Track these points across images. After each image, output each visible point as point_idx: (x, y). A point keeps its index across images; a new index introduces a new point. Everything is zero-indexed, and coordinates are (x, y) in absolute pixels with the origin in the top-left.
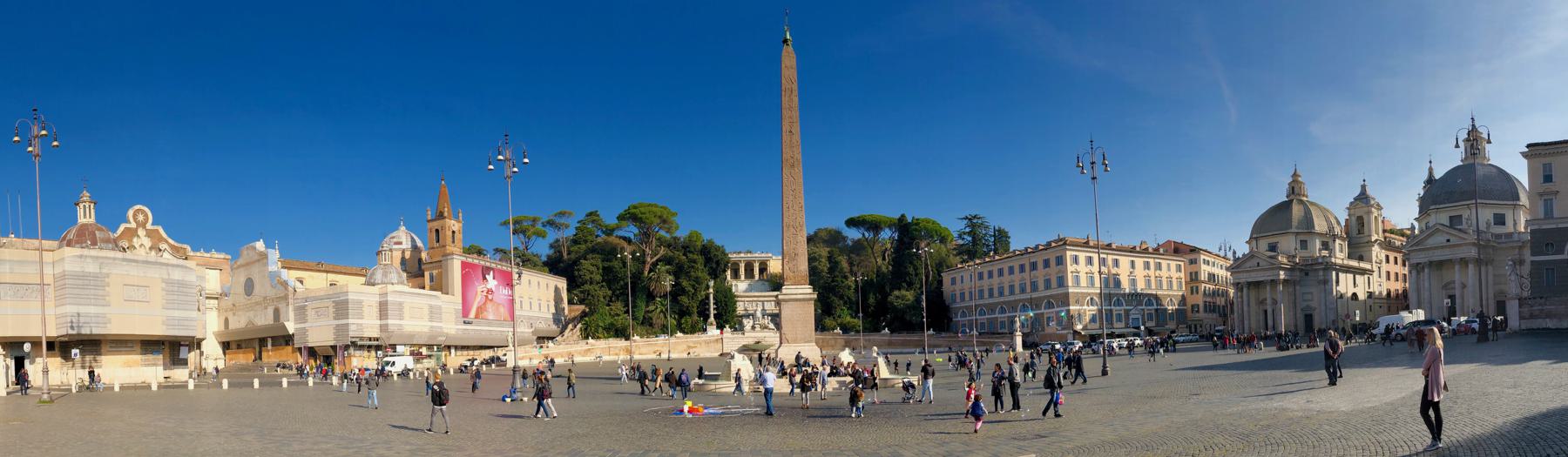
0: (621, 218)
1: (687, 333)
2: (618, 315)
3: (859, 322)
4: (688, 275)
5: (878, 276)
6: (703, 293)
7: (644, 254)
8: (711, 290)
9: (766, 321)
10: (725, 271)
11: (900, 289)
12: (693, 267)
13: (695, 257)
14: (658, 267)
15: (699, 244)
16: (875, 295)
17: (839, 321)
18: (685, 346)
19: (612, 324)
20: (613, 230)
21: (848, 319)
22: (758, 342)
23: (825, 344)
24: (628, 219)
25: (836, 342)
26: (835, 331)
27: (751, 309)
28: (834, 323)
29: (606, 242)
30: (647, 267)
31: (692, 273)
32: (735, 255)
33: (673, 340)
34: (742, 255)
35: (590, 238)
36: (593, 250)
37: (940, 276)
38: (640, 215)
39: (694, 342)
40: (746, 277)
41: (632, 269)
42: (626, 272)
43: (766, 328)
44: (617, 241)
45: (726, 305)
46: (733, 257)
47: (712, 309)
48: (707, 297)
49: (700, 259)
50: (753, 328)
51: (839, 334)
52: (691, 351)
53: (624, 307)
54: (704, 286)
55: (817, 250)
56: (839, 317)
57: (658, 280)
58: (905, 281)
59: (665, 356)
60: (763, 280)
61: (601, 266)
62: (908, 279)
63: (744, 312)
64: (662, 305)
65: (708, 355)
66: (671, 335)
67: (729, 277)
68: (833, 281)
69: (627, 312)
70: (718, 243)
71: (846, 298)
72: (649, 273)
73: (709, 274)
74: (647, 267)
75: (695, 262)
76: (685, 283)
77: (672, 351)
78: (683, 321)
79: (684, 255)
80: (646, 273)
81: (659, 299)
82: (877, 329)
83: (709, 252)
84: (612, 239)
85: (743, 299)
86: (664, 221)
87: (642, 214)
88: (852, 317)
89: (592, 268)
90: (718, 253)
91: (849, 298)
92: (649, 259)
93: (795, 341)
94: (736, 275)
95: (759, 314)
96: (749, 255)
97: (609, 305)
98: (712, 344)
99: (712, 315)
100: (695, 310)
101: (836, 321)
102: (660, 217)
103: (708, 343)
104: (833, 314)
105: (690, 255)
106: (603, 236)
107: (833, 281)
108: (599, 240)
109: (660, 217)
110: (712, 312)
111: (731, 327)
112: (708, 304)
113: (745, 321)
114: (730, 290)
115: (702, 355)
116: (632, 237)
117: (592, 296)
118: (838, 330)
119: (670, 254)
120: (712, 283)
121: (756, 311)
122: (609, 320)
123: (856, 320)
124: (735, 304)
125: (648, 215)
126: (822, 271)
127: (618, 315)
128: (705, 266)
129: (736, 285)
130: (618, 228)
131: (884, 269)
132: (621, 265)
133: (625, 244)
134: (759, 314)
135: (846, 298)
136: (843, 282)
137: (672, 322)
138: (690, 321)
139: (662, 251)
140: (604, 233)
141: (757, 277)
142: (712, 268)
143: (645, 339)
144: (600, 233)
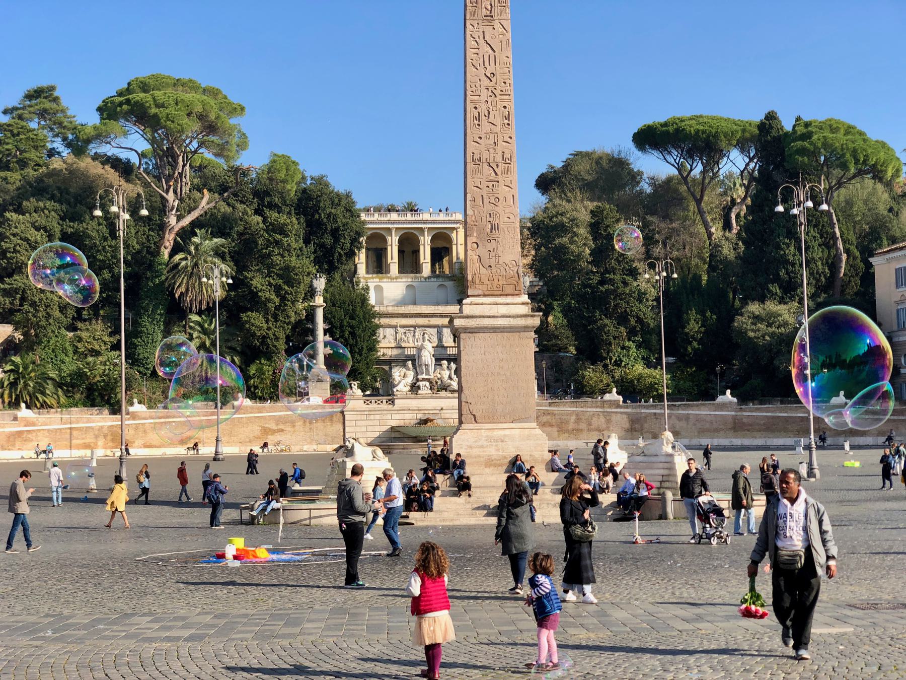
0: (108, 111)
1: (262, 399)
2: (97, 353)
3: (662, 377)
4: (264, 259)
5: (712, 268)
6: (300, 306)
7: (161, 208)
8: (319, 300)
9: (446, 374)
10: (351, 254)
11: (762, 300)
12: (278, 243)
13: (283, 219)
14: (196, 240)
15: (292, 188)
16: (703, 313)
17: (617, 374)
18: (256, 429)
19: (79, 375)
20: (88, 141)
21: (640, 368)
22: (425, 422)
23: (583, 426)
24: (126, 116)
25: (609, 421)
26: (607, 397)
27: (410, 343)
28: (606, 379)
29: (73, 173)
30: (169, 239)
31: (277, 259)
32: (376, 216)
33: (226, 413)
34: (394, 216)
35: (32, 155)
36: (39, 189)
37: (869, 266)
38: (153, 110)
39: (278, 420)
40: (402, 270)
41: (133, 242)
42: (116, 249)
43: (445, 388)
44: (95, 169)
45: (353, 334)
46: (372, 221)
48: (311, 316)
49: (295, 224)
50: (414, 388)
51: (615, 404)
52: (271, 440)
53: (111, 335)
54: (302, 288)
55: (568, 207)
56: (618, 364)
57: (194, 273)
58: (777, 279)
59: (207, 450)
60: (442, 276)
61: (57, 230)
62: (782, 273)
63: (396, 352)
64: (204, 331)
65: (309, 448)
66: (224, 403)
67: (362, 269)
68: (602, 282)
69: (116, 347)
70: (338, 185)
71: (633, 322)
72: (172, 255)
73: (317, 261)
74: (169, 239)
75: (282, 230)
76: (258, 282)
77: (224, 439)
78: (252, 370)
79: (258, 212)
80: (166, 253)
81: (195, 318)
82: (708, 395)
83: (316, 209)
84: (86, 164)
85: (394, 321)
86: (211, 128)
87: (158, 106)
88: (649, 365)
89: (33, 235)
90: (338, 211)
91: (640, 320)
92: (172, 220)
94: (378, 265)
95: (427, 357)
96: (409, 217)
97: (72, 328)
98: (320, 424)
99: (321, 358)
100: (282, 345)
101: (610, 373)
102: (201, 117)
103: (309, 419)
104: (603, 359)
105: (273, 215)
106: (65, 152)
107: (602, 282)
108: (56, 164)
109: (201, 117)
111: (363, 388)
112: (313, 332)
113: (397, 373)
114: (364, 300)
115: (295, 450)
116: (135, 159)
117: (34, 304)
118: (614, 396)
119: (225, 208)
120: (320, 283)
121: (420, 349)
122: (70, 365)
123: (656, 373)
124: (374, 333)
125: (171, 110)
126: (579, 256)
127: (97, 353)
128: (307, 242)
129: (379, 289)
130: (100, 136)
131: (727, 251)
132: (105, 231)
133: (112, 176)
134: (427, 357)
135: (633, 322)
136: (625, 284)
138: (268, 369)
139: (206, 202)
140: (69, 145)
141: (426, 269)
142: (322, 246)
143: (160, 411)
144: (58, 145)
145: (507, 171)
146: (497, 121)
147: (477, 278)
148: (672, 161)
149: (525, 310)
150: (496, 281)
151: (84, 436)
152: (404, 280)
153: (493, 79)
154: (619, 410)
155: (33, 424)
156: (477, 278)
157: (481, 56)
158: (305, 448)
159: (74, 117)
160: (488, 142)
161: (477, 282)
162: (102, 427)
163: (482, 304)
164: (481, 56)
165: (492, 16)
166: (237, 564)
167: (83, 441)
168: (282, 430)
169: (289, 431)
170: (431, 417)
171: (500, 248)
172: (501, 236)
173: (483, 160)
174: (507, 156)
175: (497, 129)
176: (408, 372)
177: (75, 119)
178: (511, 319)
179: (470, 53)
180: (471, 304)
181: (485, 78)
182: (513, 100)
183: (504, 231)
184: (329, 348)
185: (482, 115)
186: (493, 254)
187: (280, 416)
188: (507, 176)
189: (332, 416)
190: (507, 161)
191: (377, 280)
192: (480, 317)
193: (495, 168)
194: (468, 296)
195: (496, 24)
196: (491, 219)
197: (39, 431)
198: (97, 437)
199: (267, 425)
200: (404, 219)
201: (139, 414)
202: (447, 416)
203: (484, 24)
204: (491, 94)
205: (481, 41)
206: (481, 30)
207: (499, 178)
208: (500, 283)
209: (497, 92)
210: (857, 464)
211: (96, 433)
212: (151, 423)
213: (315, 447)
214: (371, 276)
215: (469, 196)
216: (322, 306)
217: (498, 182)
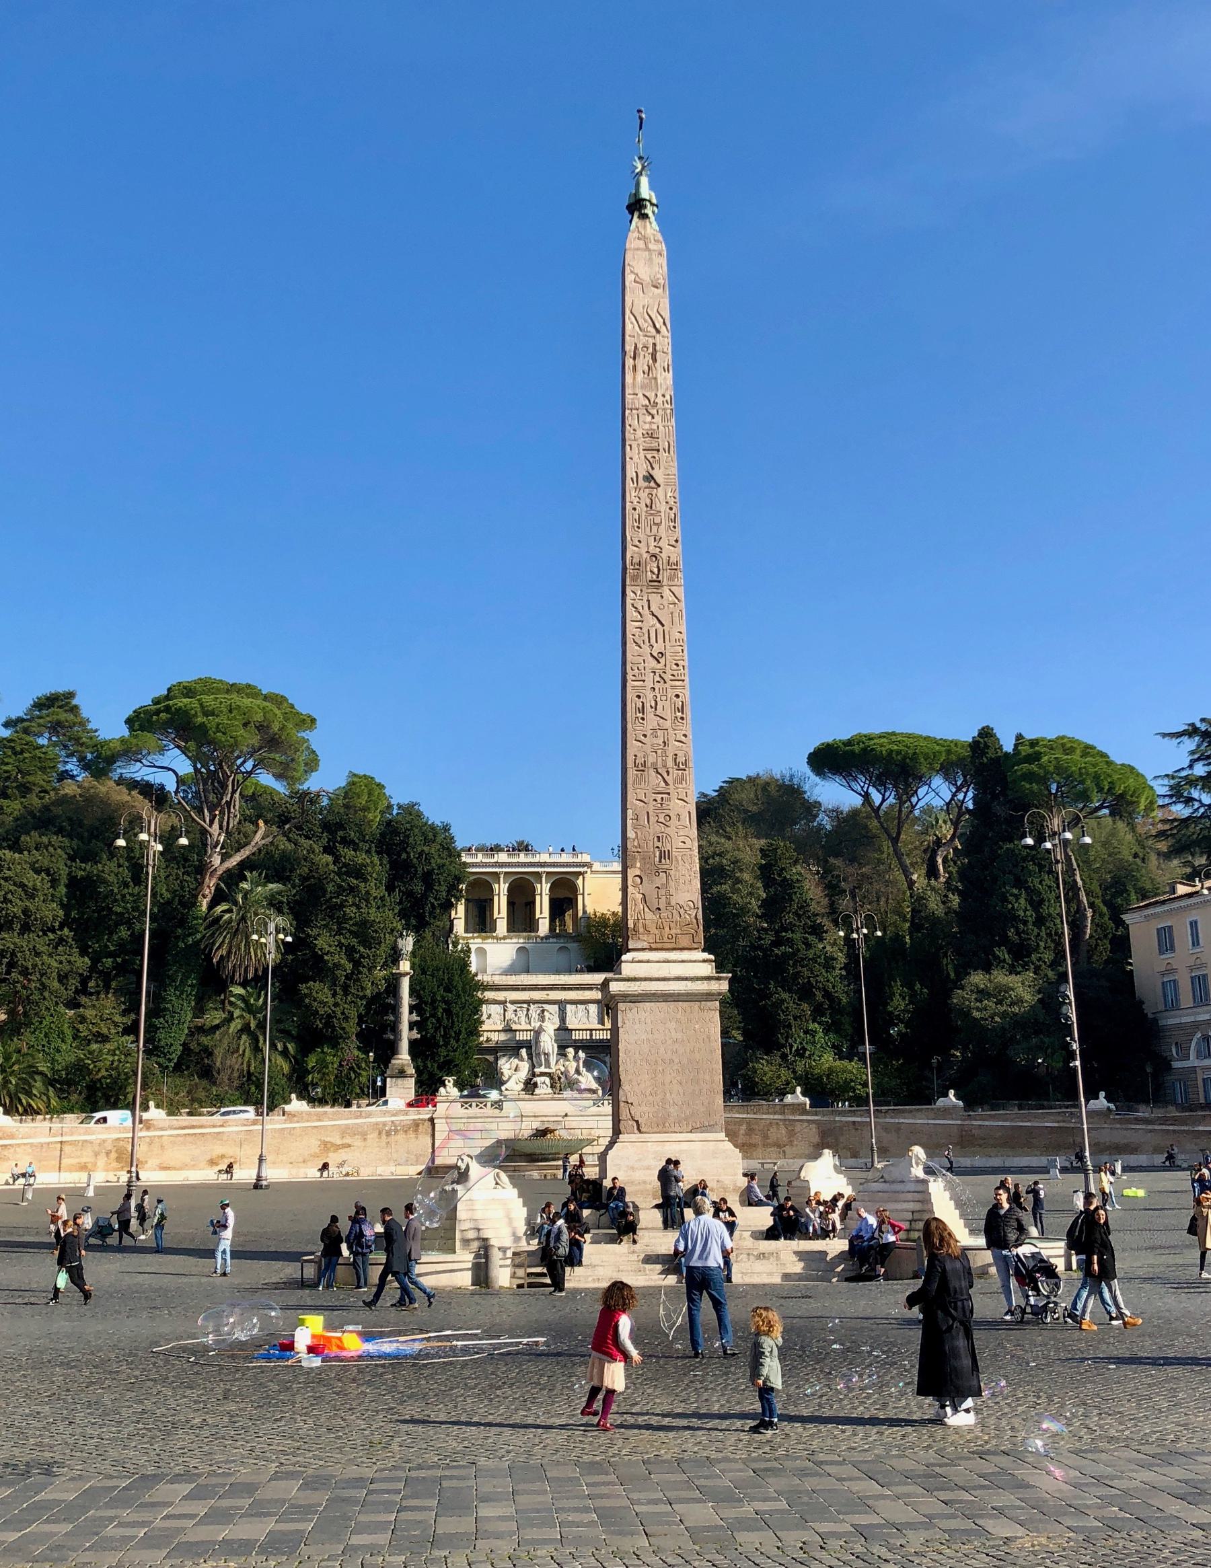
0: (140, 721)
1: (322, 1102)
2: (103, 1039)
3: (861, 1072)
4: (334, 910)
6: (380, 973)
7: (201, 841)
8: (405, 966)
9: (572, 1066)
10: (448, 906)
11: (987, 969)
12: (353, 890)
13: (361, 858)
14: (245, 885)
15: (375, 817)
16: (911, 988)
17: (800, 1069)
18: (314, 1144)
19: (79, 1068)
20: (111, 760)
21: (828, 1060)
22: (543, 1133)
23: (757, 1139)
24: (164, 727)
25: (792, 1134)
26: (789, 1098)
27: (523, 1026)
28: (785, 1074)
29: (90, 799)
30: (210, 885)
31: (350, 911)
32: (480, 858)
33: (274, 1122)
34: (503, 857)
35: (39, 778)
36: (43, 821)
38: (200, 719)
39: (344, 1131)
40: (512, 928)
41: (163, 889)
42: (140, 898)
43: (572, 1085)
44: (122, 795)
45: (448, 1012)
46: (476, 862)
47: (405, 1027)
48: (393, 987)
49: (376, 866)
50: (530, 1086)
51: (800, 1108)
52: (333, 1159)
53: (124, 1013)
54: (384, 950)
56: (800, 1053)
57: (240, 930)
58: (1005, 941)
59: (245, 1174)
60: (564, 935)
61: (64, 873)
62: (1011, 933)
63: (503, 1037)
64: (249, 1009)
65: (386, 1171)
66: (271, 1109)
67: (459, 926)
68: (778, 943)
69: (132, 1029)
70: (434, 815)
71: (819, 996)
72: (212, 905)
73: (403, 915)
74: (210, 885)
75: (358, 872)
76: (324, 941)
77: (269, 1158)
78: (311, 1061)
79: (327, 850)
80: (205, 904)
81: (239, 990)
82: (921, 1096)
83: (404, 845)
84: (107, 788)
85: (500, 995)
86: (273, 742)
87: (206, 714)
88: (840, 1055)
89: (32, 879)
90: (433, 849)
91: (827, 995)
92: (216, 860)
93: (662, 1125)
94: (481, 922)
95: (548, 1043)
96: (522, 858)
97: (73, 1004)
98: (401, 1137)
99: (404, 1045)
100: (352, 1028)
101: (790, 1066)
102: (260, 727)
103: (387, 1132)
104: (780, 1047)
105: (348, 853)
106: (82, 776)
107: (778, 943)
108: (69, 788)
109: (260, 727)
110: (406, 1035)
111: (460, 1085)
112: (395, 1009)
113: (506, 1065)
114: (465, 965)
115: (366, 1173)
116: (171, 786)
117: (25, 972)
118: (798, 1097)
119: (284, 845)
120: (407, 944)
121: (538, 1033)
122: (68, 1054)
123: (853, 1066)
124: (476, 1010)
125: (223, 719)
126: (744, 910)
127: (103, 1039)
128: (390, 888)
129: (482, 952)
130: (129, 752)
132: (127, 875)
134: (548, 1043)
135: (819, 996)
136: (808, 946)
137: (274, 1063)
138: (333, 1061)
139: (260, 835)
140: (86, 767)
141: (544, 927)
142: (410, 894)
143: (184, 1119)
144: (72, 766)
145: (681, 780)
146: (667, 714)
147: (641, 925)
148: (860, 789)
149: (708, 969)
150: (667, 929)
151: (79, 1153)
152: (515, 940)
153: (662, 660)
154: (804, 1118)
155: (12, 1137)
156: (641, 925)
157: (645, 630)
158: (380, 1170)
159: (96, 731)
160: (655, 741)
161: (641, 930)
162: (104, 1141)
163: (648, 962)
164: (645, 630)
165: (659, 582)
166: (316, 1362)
167: (77, 1160)
168: (349, 1146)
169: (359, 1147)
170: (552, 1127)
171: (672, 884)
172: (673, 867)
173: (649, 764)
174: (681, 759)
175: (668, 724)
176: (521, 1063)
177: (97, 734)
178: (689, 983)
179: (631, 627)
180: (632, 962)
181: (651, 658)
182: (687, 687)
183: (677, 860)
184: (415, 1031)
185: (647, 706)
186: (663, 892)
187: (347, 1126)
188: (680, 786)
189: (417, 1125)
190: (681, 766)
191: (480, 940)
192: (646, 979)
193: (665, 775)
194: (629, 951)
195: (666, 592)
196: (660, 844)
197: (19, 1145)
198: (96, 1154)
199: (328, 1139)
200: (515, 860)
201: (155, 1123)
202: (574, 1125)
203: (650, 591)
204: (659, 679)
205: (646, 612)
206: (645, 598)
207: (671, 788)
208: (673, 932)
209: (667, 677)
210: (1141, 1193)
211: (97, 1149)
212: (171, 1136)
213: (393, 1169)
214: (471, 935)
215: (629, 812)
216: (408, 974)
217: (669, 794)
